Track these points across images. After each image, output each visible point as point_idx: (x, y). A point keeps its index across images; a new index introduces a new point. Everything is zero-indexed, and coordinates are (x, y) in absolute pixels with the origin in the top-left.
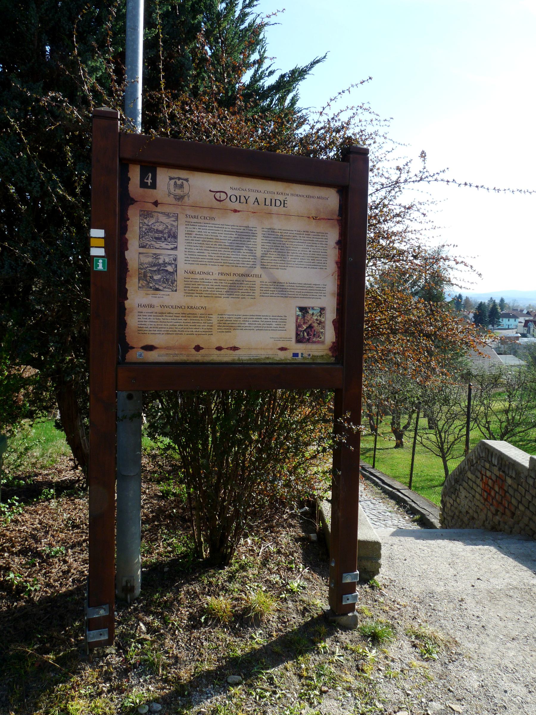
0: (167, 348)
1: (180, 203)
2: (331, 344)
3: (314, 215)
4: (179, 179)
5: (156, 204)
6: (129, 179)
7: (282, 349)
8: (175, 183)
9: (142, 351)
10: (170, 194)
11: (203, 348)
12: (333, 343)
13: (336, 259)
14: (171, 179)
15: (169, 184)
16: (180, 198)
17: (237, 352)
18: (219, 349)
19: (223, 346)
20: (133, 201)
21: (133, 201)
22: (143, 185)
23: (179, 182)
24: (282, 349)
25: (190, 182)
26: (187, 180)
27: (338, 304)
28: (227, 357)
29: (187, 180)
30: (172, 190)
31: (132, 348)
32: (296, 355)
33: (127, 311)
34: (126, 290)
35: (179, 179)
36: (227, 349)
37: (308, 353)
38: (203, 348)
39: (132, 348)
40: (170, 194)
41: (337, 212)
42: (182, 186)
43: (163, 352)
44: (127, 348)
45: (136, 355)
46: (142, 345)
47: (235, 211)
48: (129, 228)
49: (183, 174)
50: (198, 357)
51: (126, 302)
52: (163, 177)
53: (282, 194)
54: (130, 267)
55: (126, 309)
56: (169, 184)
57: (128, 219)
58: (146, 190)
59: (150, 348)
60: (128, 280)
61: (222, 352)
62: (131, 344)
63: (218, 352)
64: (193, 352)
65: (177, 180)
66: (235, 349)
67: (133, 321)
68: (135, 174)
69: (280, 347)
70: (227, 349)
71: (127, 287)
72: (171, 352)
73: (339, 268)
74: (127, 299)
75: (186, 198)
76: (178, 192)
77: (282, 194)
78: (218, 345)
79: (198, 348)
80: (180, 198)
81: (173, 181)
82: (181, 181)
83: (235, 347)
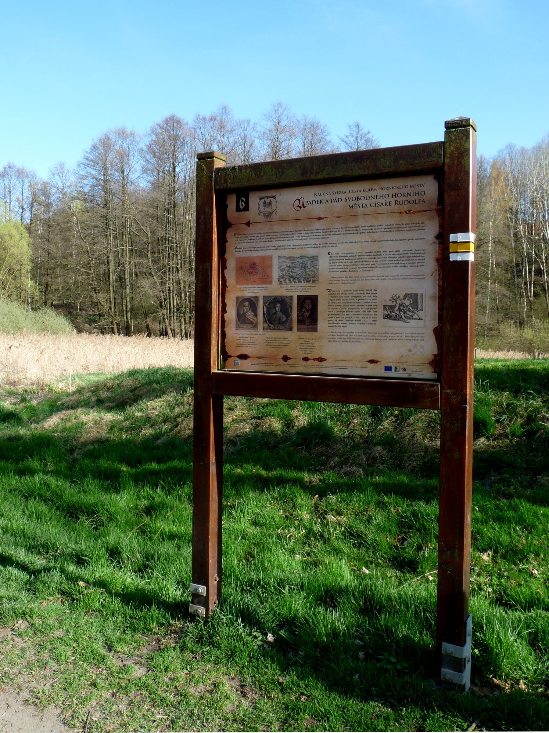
1: (268, 220)
2: (433, 357)
4: (268, 197)
5: (248, 224)
6: (227, 206)
7: (372, 362)
10: (260, 212)
11: (290, 359)
12: (435, 356)
13: (437, 255)
15: (259, 204)
16: (268, 215)
17: (323, 363)
18: (306, 359)
19: (309, 356)
20: (230, 225)
21: (230, 225)
22: (238, 209)
23: (267, 201)
24: (372, 362)
26: (274, 197)
28: (312, 368)
29: (274, 197)
30: (262, 210)
31: (230, 356)
32: (388, 369)
33: (226, 323)
35: (268, 197)
36: (314, 359)
38: (290, 359)
39: (230, 356)
40: (260, 212)
42: (270, 203)
43: (255, 361)
46: (239, 354)
47: (320, 219)
48: (228, 249)
49: (271, 193)
50: (286, 367)
51: (225, 315)
52: (254, 200)
55: (225, 321)
56: (259, 204)
57: (227, 241)
58: (240, 213)
59: (244, 357)
61: (309, 363)
63: (304, 363)
64: (282, 361)
65: (266, 199)
66: (321, 360)
70: (314, 359)
73: (440, 265)
75: (274, 214)
76: (267, 209)
78: (305, 356)
79: (286, 358)
80: (268, 215)
81: (263, 200)
82: (269, 199)
83: (321, 358)
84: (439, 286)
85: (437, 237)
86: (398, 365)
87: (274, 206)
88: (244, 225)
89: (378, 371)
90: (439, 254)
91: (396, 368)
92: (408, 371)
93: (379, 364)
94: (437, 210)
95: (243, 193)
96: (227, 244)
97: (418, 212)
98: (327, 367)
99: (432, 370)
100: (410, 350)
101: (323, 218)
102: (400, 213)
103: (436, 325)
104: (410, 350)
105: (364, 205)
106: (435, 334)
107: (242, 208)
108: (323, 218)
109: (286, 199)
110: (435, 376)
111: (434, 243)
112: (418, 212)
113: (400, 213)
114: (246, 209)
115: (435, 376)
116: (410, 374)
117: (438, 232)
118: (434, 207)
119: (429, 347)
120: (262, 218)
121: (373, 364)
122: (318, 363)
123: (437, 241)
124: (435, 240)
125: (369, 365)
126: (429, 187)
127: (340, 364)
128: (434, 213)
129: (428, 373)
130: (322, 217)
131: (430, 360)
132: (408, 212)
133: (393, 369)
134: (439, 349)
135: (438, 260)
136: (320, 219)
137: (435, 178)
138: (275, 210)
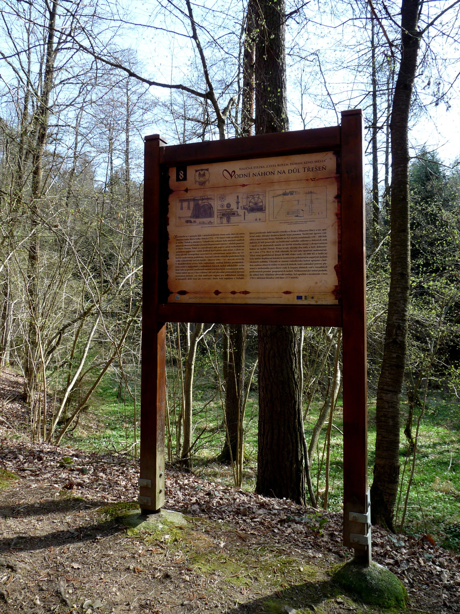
0: (196, 293)
1: (203, 187)
2: (334, 288)
3: (311, 177)
4: (202, 170)
5: (187, 190)
6: (169, 177)
7: (287, 293)
8: (200, 174)
11: (220, 293)
13: (336, 211)
14: (196, 171)
15: (195, 175)
17: (248, 295)
18: (233, 293)
19: (236, 291)
20: (171, 192)
21: (171, 192)
22: (178, 179)
23: (202, 173)
24: (287, 293)
25: (210, 170)
26: (207, 170)
28: (239, 300)
29: (207, 170)
30: (198, 179)
31: (172, 293)
32: (299, 298)
34: (168, 253)
35: (202, 170)
36: (240, 293)
38: (220, 293)
39: (172, 293)
41: (335, 171)
42: (204, 175)
43: (192, 295)
44: (169, 293)
45: (177, 298)
46: (178, 291)
47: (244, 185)
49: (204, 166)
52: (191, 171)
53: (282, 165)
54: (170, 237)
55: (167, 266)
56: (195, 175)
57: (169, 204)
59: (183, 293)
60: (169, 245)
61: (236, 295)
62: (172, 289)
63: (232, 295)
64: (214, 295)
66: (246, 293)
67: (172, 274)
68: (173, 173)
69: (285, 290)
70: (240, 293)
71: (168, 250)
72: (197, 295)
74: (168, 258)
75: (207, 183)
76: (202, 179)
77: (282, 165)
78: (232, 290)
79: (217, 293)
84: (338, 234)
85: (336, 198)
86: (307, 294)
87: (207, 177)
88: (183, 192)
89: (291, 300)
90: (338, 210)
91: (306, 297)
92: (315, 299)
93: (292, 294)
94: (336, 178)
95: (182, 167)
96: (169, 206)
97: (321, 179)
98: (250, 298)
99: (334, 297)
100: (316, 283)
102: (307, 180)
103: (337, 263)
104: (316, 283)
107: (181, 178)
109: (217, 171)
110: (336, 302)
111: (334, 202)
112: (321, 179)
113: (307, 180)
114: (185, 179)
115: (336, 302)
116: (317, 302)
117: (336, 194)
118: (334, 175)
119: (330, 280)
120: (197, 186)
121: (288, 296)
122: (243, 295)
123: (336, 201)
124: (334, 199)
125: (284, 295)
126: (329, 160)
127: (261, 295)
128: (334, 180)
129: (330, 300)
133: (303, 298)
134: (339, 281)
135: (337, 215)
136: (244, 185)
137: (334, 154)
138: (208, 180)
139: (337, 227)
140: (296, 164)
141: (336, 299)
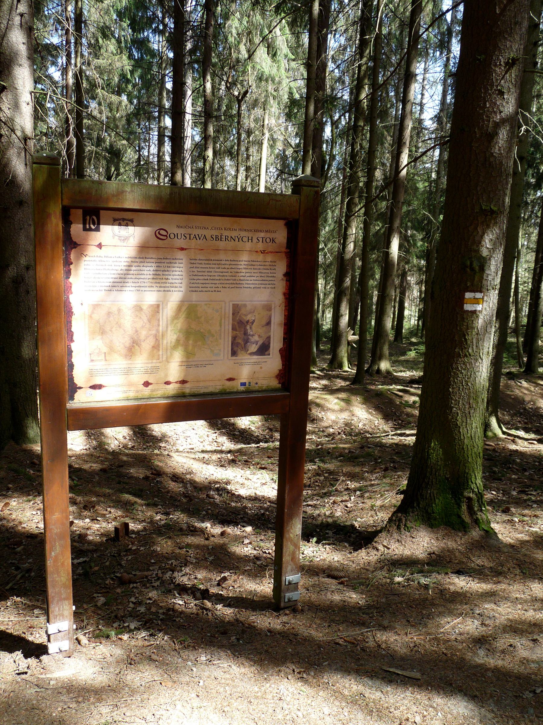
2: (278, 372)
3: (262, 249)
7: (230, 379)
9: (91, 390)
11: (151, 384)
12: (280, 371)
13: (284, 290)
19: (171, 380)
27: (285, 333)
31: (80, 388)
37: (255, 382)
38: (151, 384)
39: (80, 388)
41: (285, 245)
46: (91, 385)
53: (230, 229)
73: (286, 299)
101: (186, 249)
103: (282, 346)
105: (192, 236)
106: (280, 353)
108: (186, 249)
130: (185, 247)
131: (276, 374)
132: (263, 252)
135: (284, 294)
139: (284, 308)
140: (245, 230)
141: (279, 383)
